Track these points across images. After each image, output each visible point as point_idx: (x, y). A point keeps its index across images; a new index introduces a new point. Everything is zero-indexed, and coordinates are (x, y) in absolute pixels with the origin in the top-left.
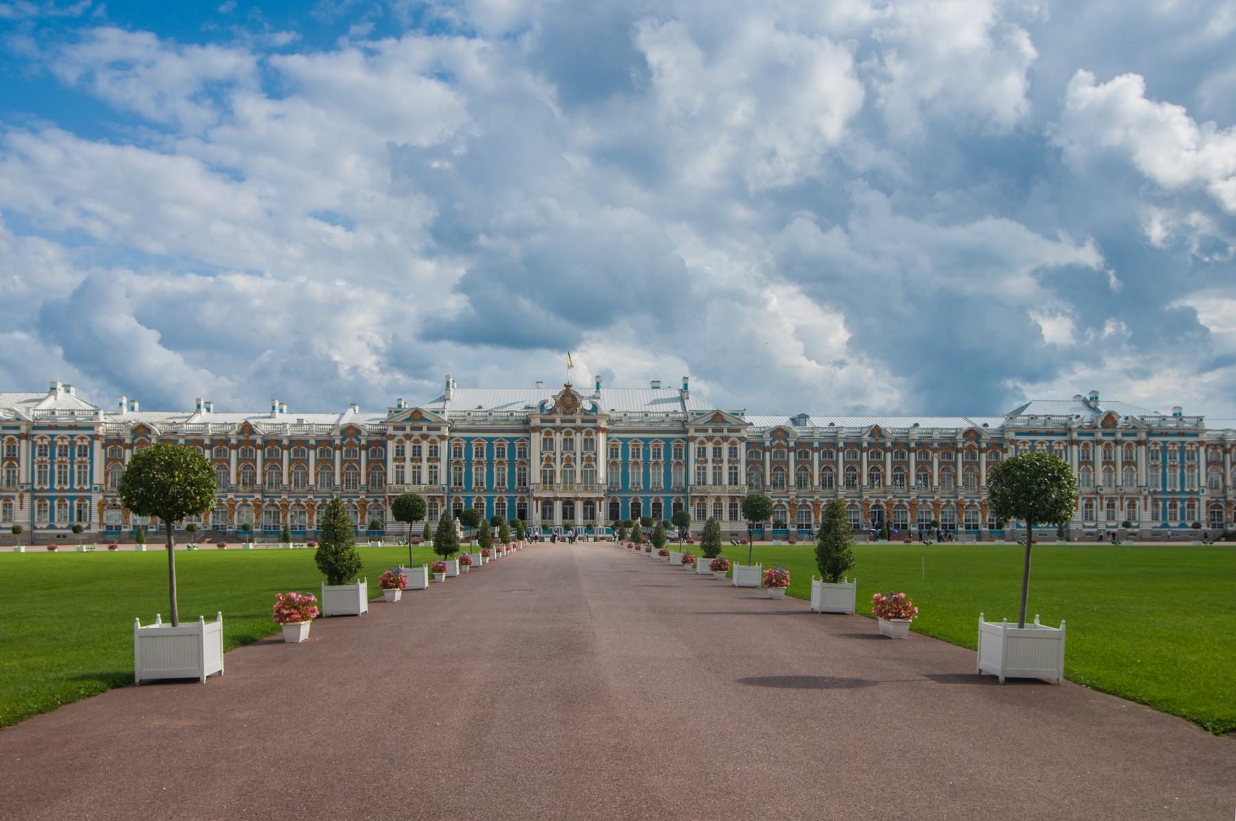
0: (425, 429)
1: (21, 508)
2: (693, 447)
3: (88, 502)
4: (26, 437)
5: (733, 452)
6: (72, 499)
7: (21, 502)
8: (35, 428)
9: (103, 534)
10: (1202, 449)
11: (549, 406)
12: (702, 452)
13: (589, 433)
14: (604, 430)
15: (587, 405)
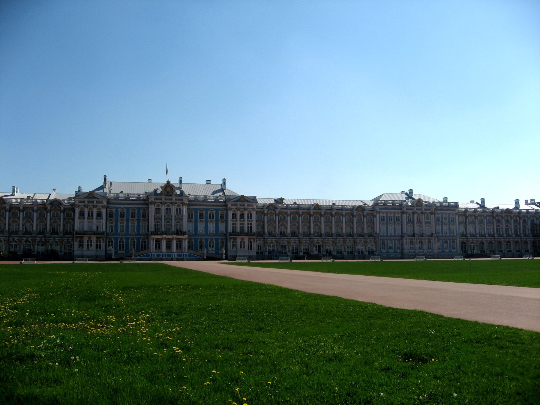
0: (95, 202)
2: (230, 213)
5: (250, 216)
10: (457, 217)
11: (158, 192)
12: (234, 216)
13: (179, 206)
14: (186, 204)
15: (178, 192)
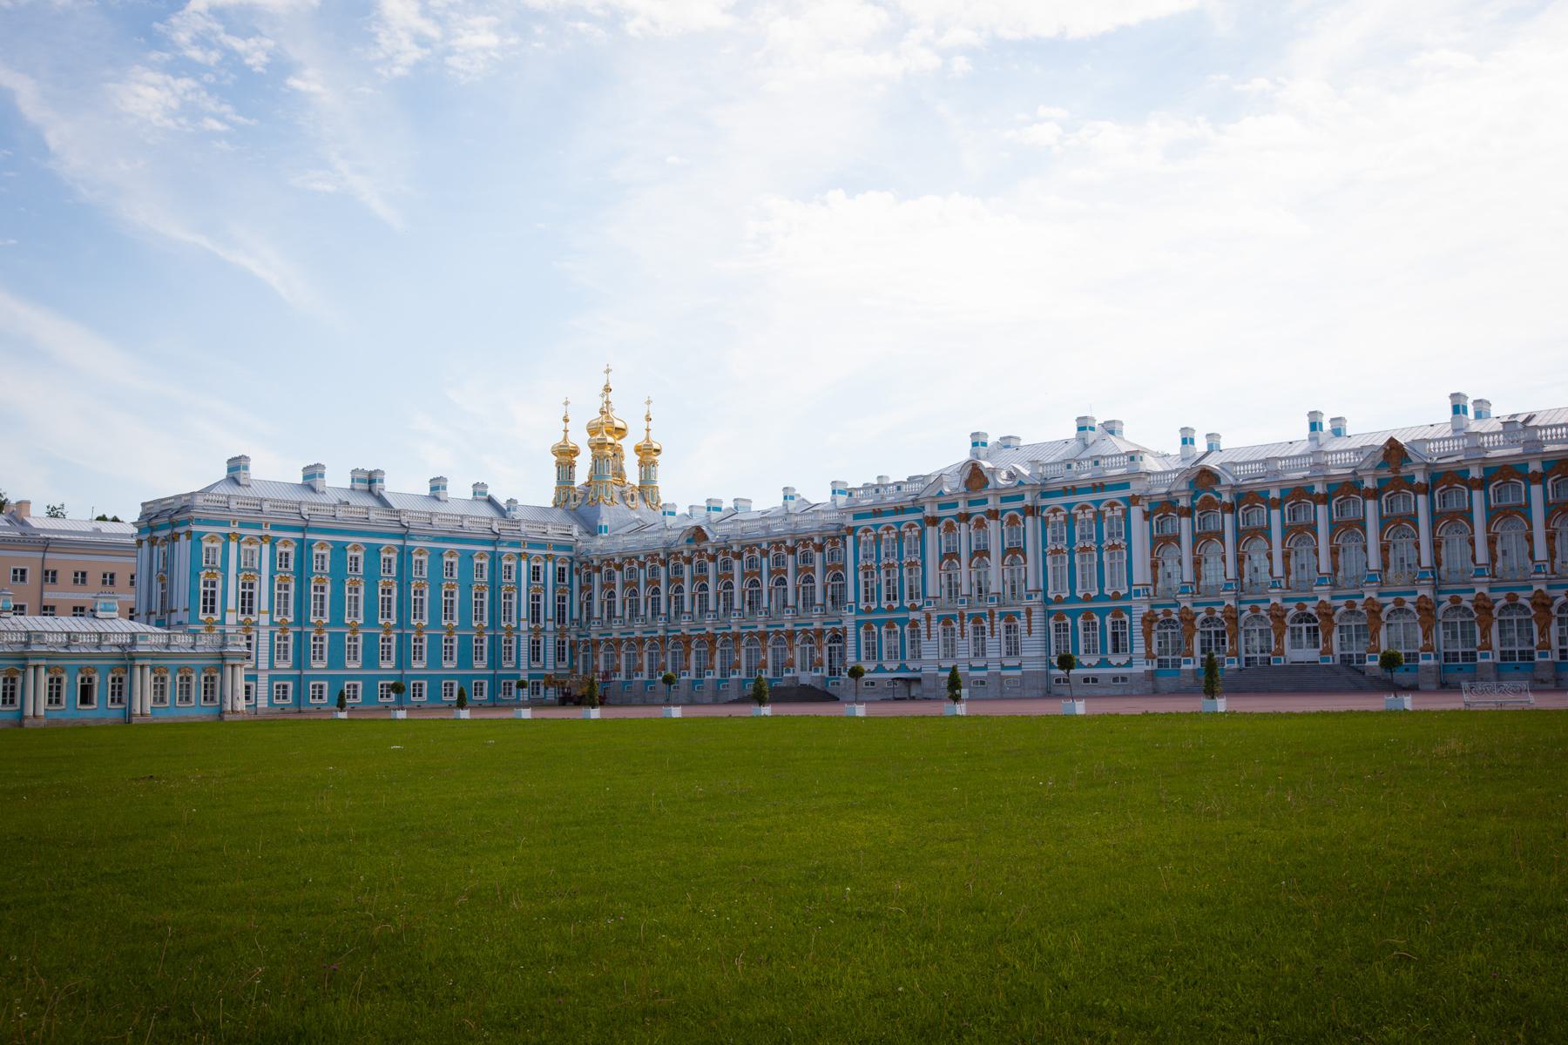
1: (1030, 632)
3: (1126, 618)
4: (1031, 511)
6: (1103, 613)
7: (1029, 622)
8: (1044, 495)
9: (1151, 675)
